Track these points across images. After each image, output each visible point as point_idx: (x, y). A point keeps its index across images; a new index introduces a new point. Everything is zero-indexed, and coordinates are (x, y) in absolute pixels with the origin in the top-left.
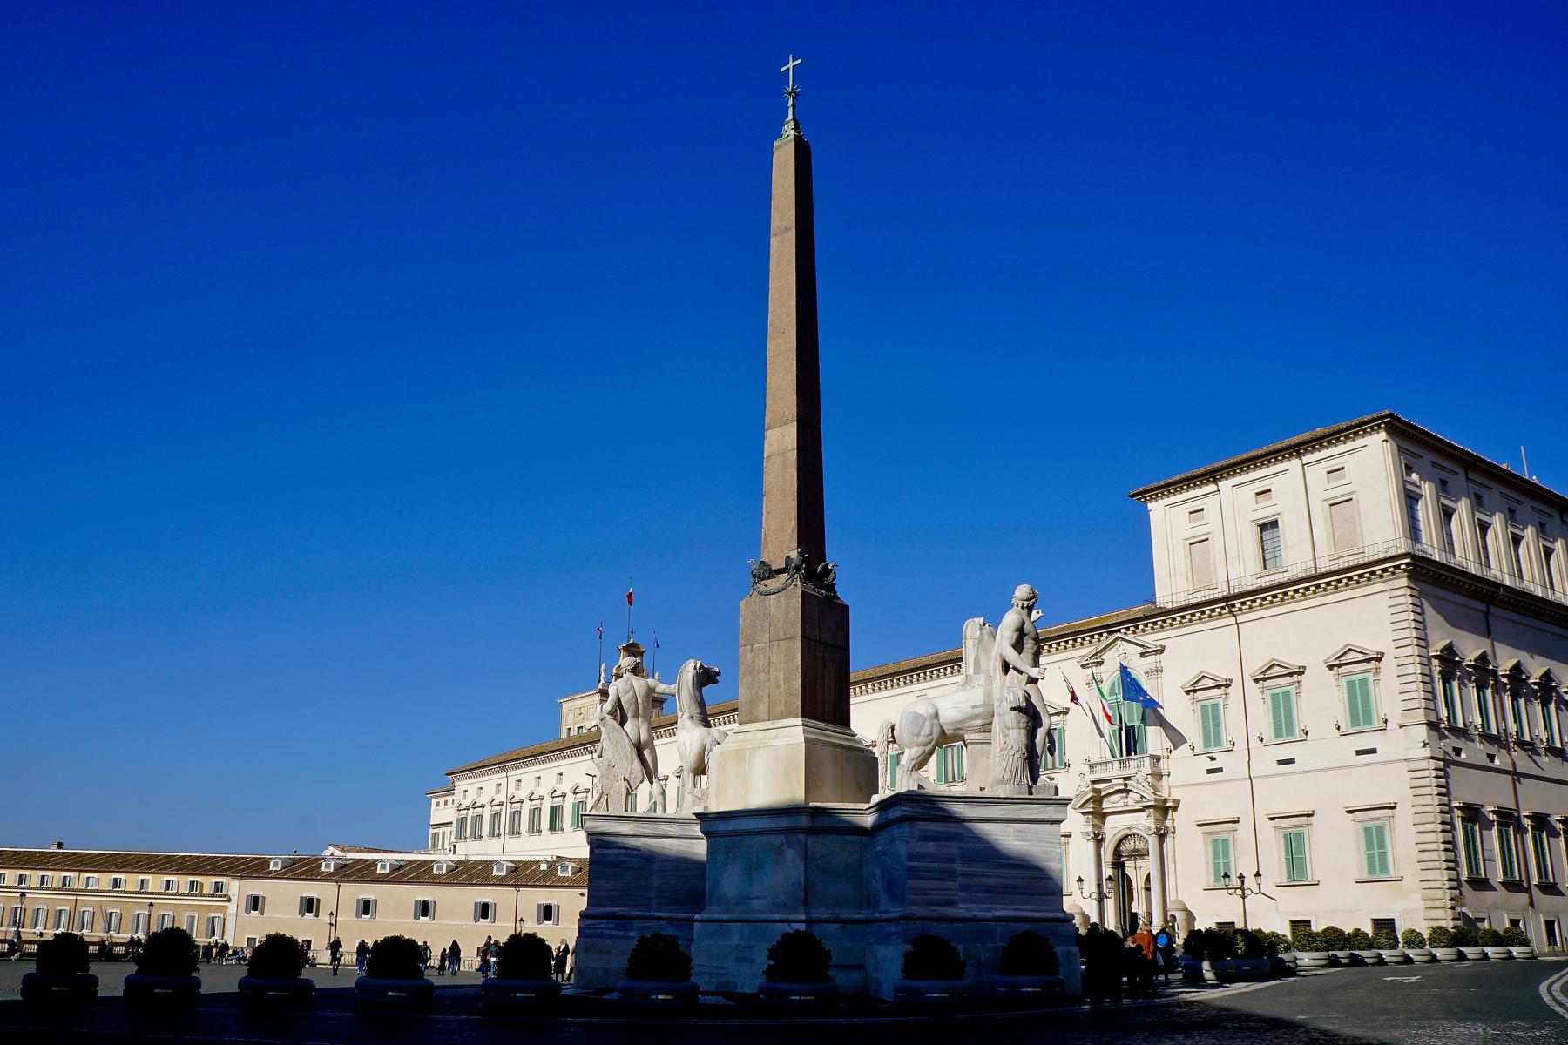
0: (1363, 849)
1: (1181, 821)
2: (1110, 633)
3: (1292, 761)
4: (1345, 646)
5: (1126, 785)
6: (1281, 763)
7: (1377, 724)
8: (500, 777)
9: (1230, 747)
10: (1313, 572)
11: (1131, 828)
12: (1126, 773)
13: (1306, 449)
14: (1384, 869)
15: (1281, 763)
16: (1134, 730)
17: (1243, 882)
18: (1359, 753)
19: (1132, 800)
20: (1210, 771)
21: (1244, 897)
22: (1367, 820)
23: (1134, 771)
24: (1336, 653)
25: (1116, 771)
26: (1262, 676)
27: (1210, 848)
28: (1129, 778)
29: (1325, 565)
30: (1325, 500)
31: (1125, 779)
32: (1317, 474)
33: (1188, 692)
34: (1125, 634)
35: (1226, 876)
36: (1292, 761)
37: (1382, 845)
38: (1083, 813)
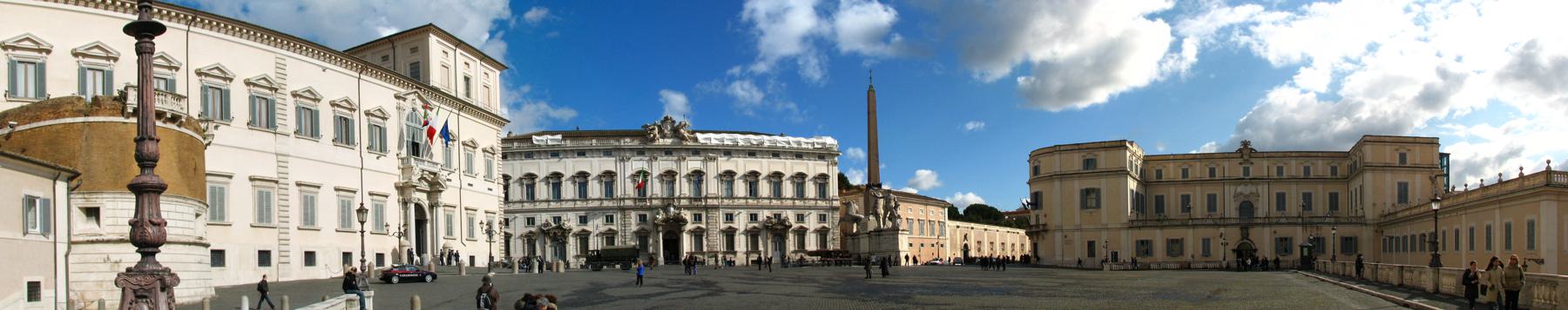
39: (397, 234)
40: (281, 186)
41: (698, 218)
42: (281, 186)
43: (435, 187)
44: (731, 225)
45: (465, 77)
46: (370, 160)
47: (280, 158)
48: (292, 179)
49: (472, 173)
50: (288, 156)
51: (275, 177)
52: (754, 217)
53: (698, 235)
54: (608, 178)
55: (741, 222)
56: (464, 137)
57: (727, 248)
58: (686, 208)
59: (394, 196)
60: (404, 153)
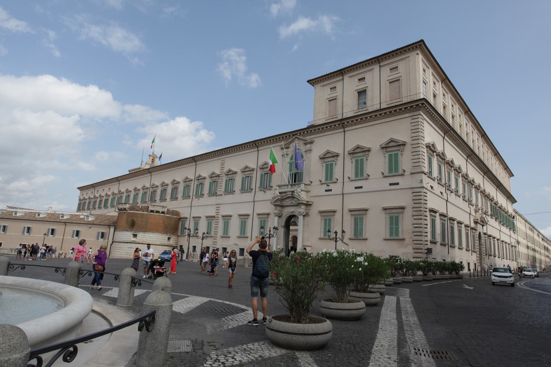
0: (388, 225)
1: (314, 211)
2: (293, 135)
3: (361, 187)
4: (390, 139)
5: (292, 194)
6: (356, 188)
7: (400, 172)
8: (92, 190)
9: (336, 181)
10: (379, 109)
11: (293, 212)
12: (293, 189)
13: (382, 59)
14: (397, 234)
15: (356, 188)
16: (298, 174)
17: (336, 235)
18: (391, 184)
19: (294, 202)
20: (326, 191)
21: (336, 242)
22: (392, 213)
23: (295, 189)
24: (386, 142)
25: (289, 189)
26: (352, 152)
27: (323, 222)
28: (293, 192)
29: (384, 106)
30: (388, 80)
32: (386, 71)
33: (321, 158)
34: (299, 135)
35: (329, 231)
36: (361, 187)
37: (397, 224)
38: (274, 205)
39: (201, 238)
42: (216, 218)
46: (260, 195)
47: (218, 206)
50: (220, 204)
51: (213, 214)
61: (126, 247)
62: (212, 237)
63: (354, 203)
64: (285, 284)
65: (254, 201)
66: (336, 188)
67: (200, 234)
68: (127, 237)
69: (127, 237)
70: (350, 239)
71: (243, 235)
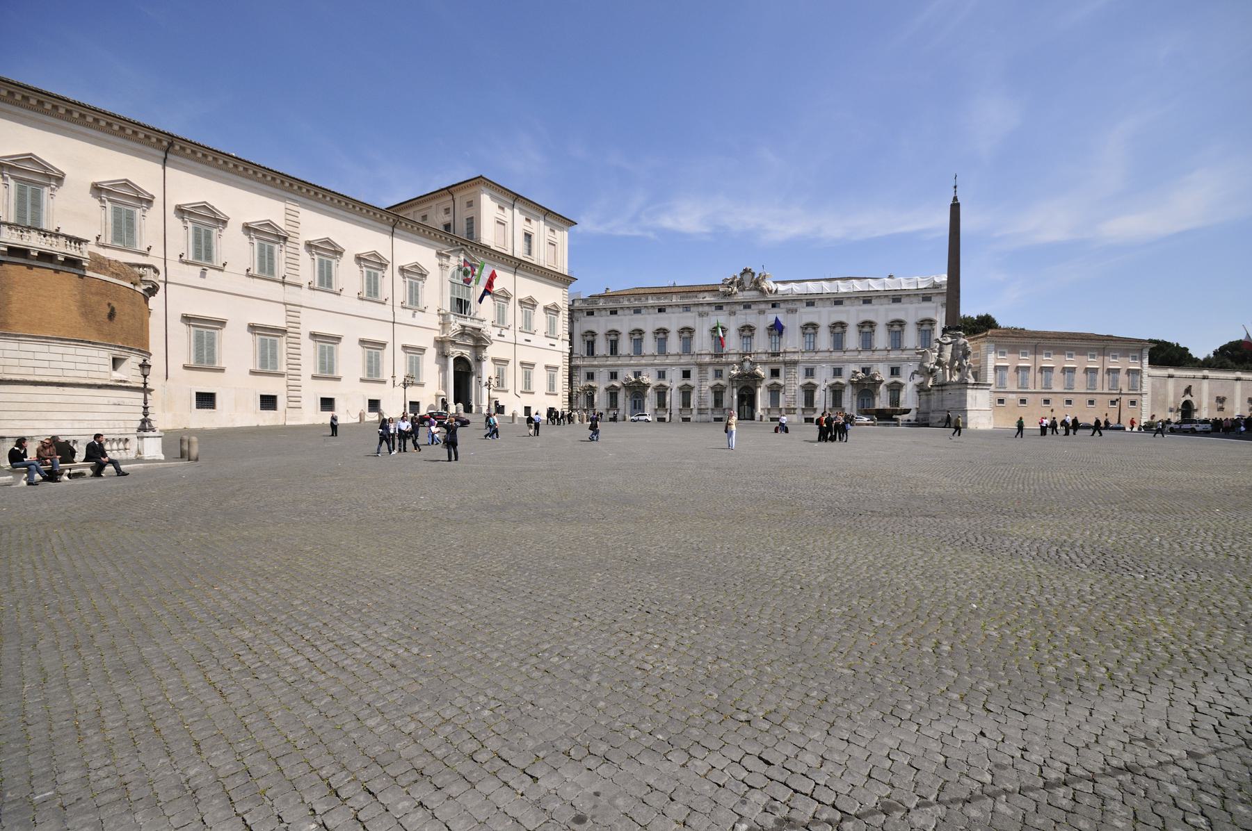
3: (529, 341)
20: (499, 335)
29: (546, 267)
31: (473, 328)
36: (529, 341)
40: (290, 334)
41: (775, 373)
42: (290, 334)
43: (479, 341)
44: (811, 380)
45: (526, 234)
46: (404, 316)
47: (289, 307)
48: (305, 330)
49: (530, 329)
50: (301, 306)
51: (281, 324)
52: (838, 372)
53: (775, 391)
54: (687, 333)
55: (823, 379)
56: (523, 295)
57: (806, 404)
58: (765, 363)
59: (432, 353)
60: (447, 307)
61: (105, 401)
62: (282, 375)
63: (525, 355)
64: (819, 422)
65: (394, 323)
66: (509, 335)
67: (400, 379)
68: (95, 368)
69: (95, 368)
70: (521, 392)
71: (551, 392)
